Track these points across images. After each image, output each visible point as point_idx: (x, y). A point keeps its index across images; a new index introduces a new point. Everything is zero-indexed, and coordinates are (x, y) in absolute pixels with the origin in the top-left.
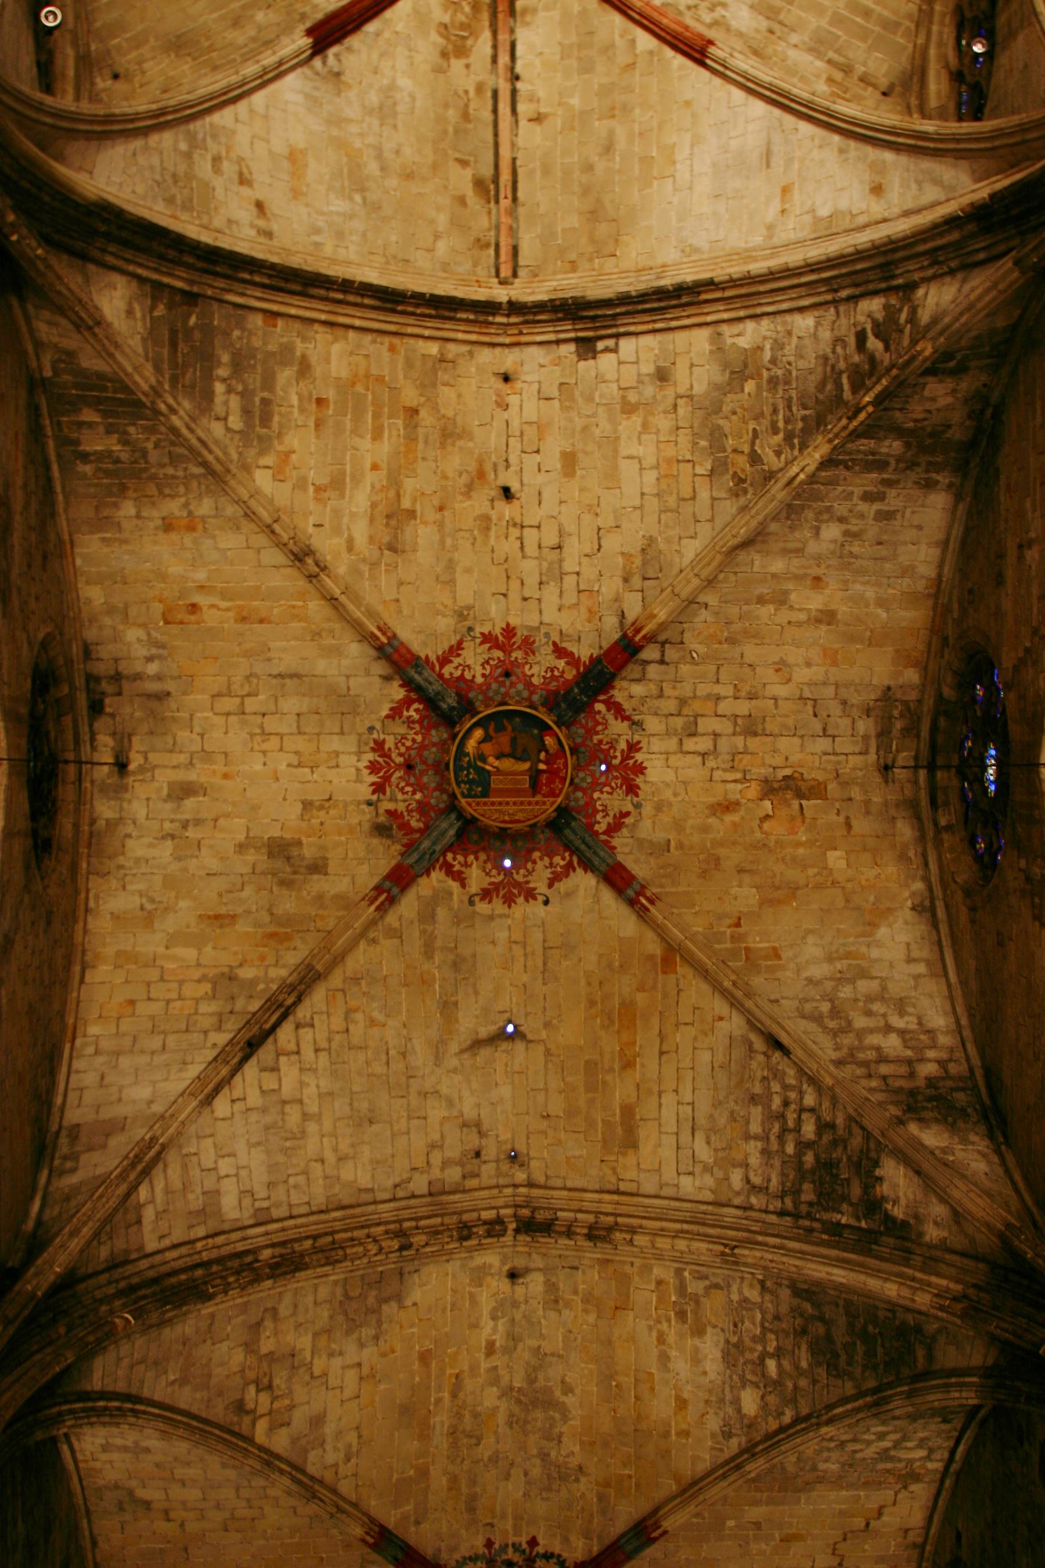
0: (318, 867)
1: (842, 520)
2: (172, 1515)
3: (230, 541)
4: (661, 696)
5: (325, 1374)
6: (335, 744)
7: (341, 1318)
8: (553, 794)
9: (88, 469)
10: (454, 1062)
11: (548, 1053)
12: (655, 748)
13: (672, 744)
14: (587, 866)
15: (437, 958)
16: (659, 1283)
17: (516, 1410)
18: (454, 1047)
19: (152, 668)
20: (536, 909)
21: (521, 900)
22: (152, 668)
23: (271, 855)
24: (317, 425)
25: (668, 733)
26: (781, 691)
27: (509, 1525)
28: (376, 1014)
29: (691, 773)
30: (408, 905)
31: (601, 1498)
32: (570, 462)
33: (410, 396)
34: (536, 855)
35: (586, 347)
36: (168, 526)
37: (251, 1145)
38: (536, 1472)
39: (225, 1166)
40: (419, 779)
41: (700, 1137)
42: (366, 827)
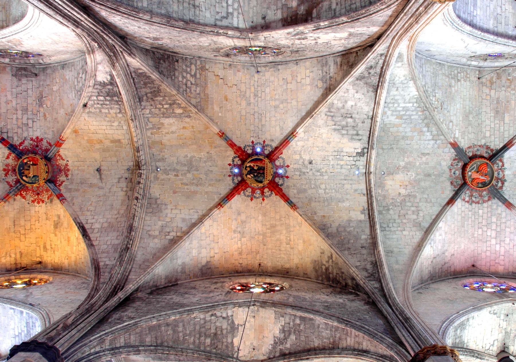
0: (59, 217)
2: (212, 255)
5: (171, 218)
7: (157, 214)
8: (38, 160)
10: (104, 184)
11: (102, 161)
12: (32, 134)
15: (80, 188)
16: (152, 134)
17: (194, 169)
18: (100, 184)
20: (70, 163)
21: (68, 167)
23: (57, 228)
28: (89, 204)
29: (38, 125)
30: (66, 195)
34: (57, 163)
37: (107, 236)
38: (210, 164)
39: (109, 243)
40: (41, 192)
41: (113, 124)
42: (51, 205)
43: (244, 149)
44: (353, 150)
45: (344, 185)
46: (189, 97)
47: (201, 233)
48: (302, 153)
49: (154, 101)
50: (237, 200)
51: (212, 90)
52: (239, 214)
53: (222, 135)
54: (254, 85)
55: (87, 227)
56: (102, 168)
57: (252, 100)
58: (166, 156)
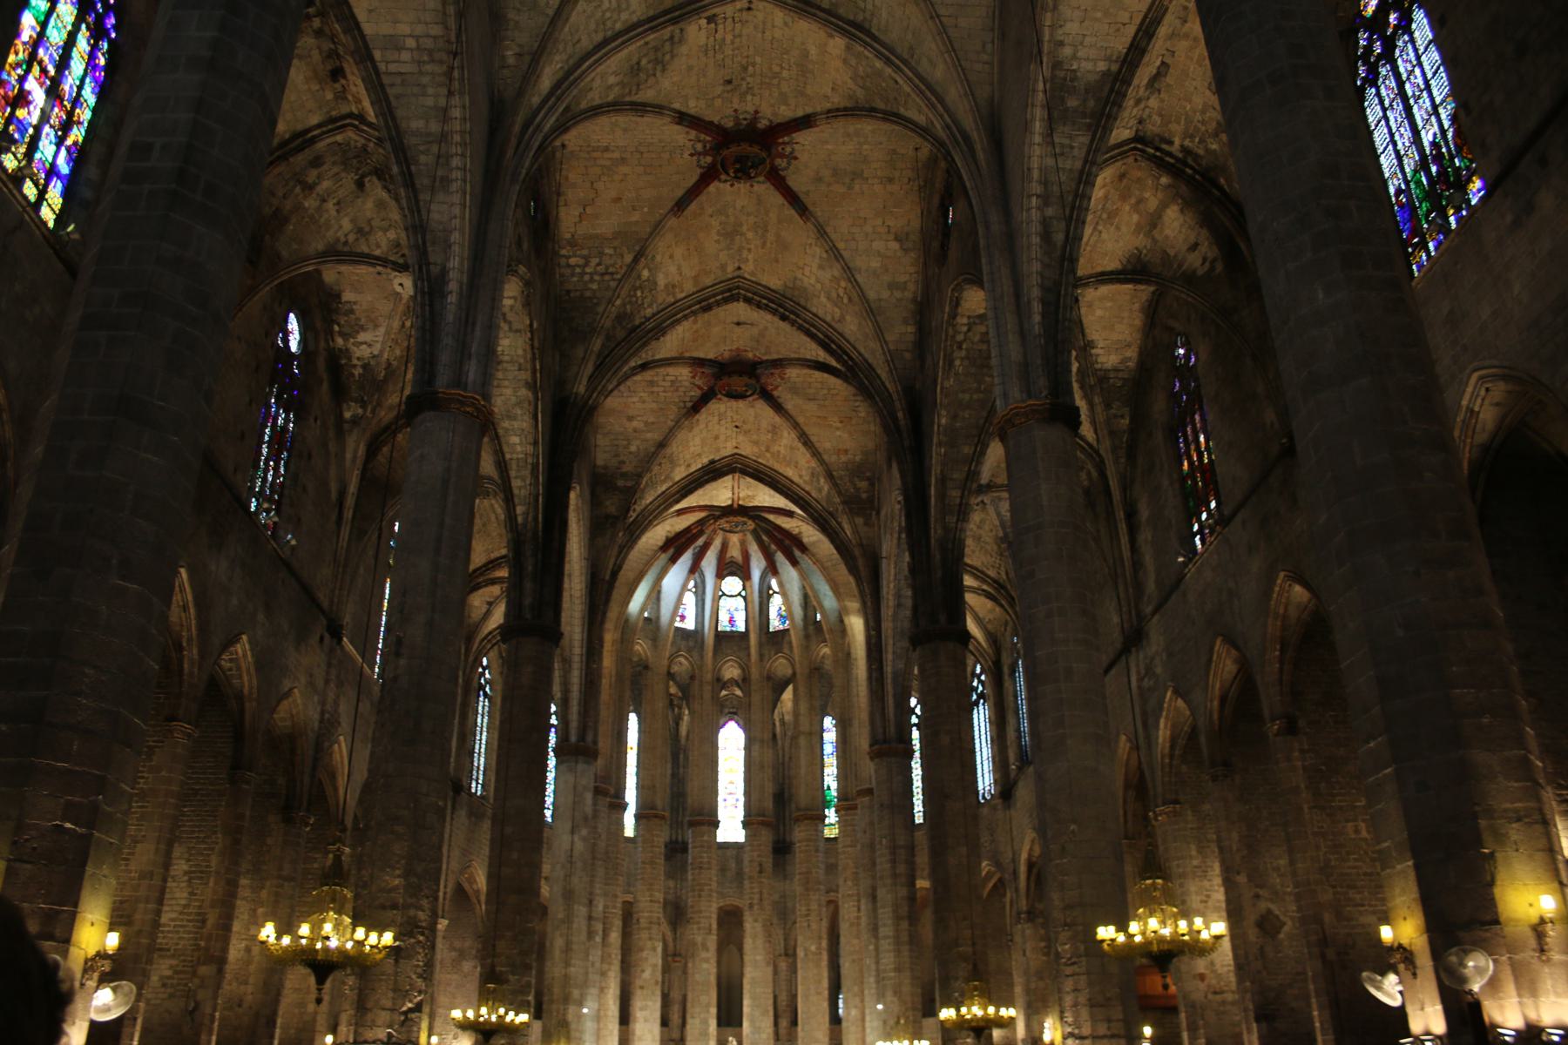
1: (630, 453)
3: (828, 445)
4: (685, 392)
6: (797, 380)
9: (868, 474)
11: (724, 323)
13: (679, 378)
14: (710, 360)
16: (682, 292)
19: (857, 404)
22: (857, 404)
24: (797, 463)
25: (681, 381)
26: (642, 394)
27: (742, 190)
31: (703, 208)
32: (717, 438)
33: (768, 455)
35: (712, 462)
36: (846, 451)
38: (731, 211)
43: (704, 167)
44: (703, 31)
45: (773, 38)
46: (621, 267)
47: (845, 250)
48: (711, 96)
49: (632, 314)
50: (797, 182)
51: (607, 224)
52: (819, 179)
53: (680, 206)
54: (588, 152)
55: (821, 360)
56: (735, 320)
57: (616, 155)
58: (718, 265)
